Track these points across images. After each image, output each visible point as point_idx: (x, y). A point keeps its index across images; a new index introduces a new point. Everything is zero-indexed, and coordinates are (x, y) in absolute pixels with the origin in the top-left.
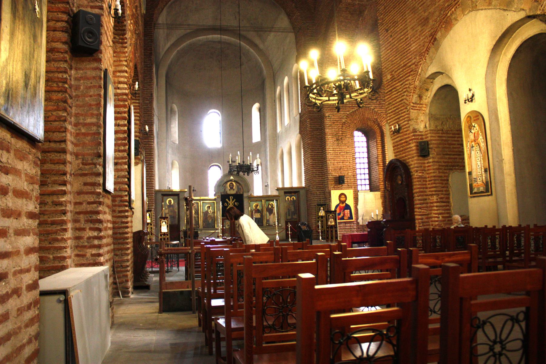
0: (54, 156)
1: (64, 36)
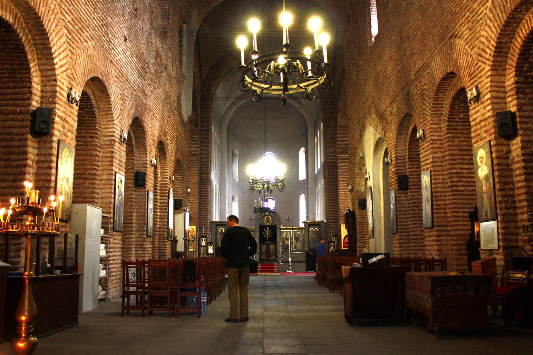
0: (129, 225)
1: (132, 182)
